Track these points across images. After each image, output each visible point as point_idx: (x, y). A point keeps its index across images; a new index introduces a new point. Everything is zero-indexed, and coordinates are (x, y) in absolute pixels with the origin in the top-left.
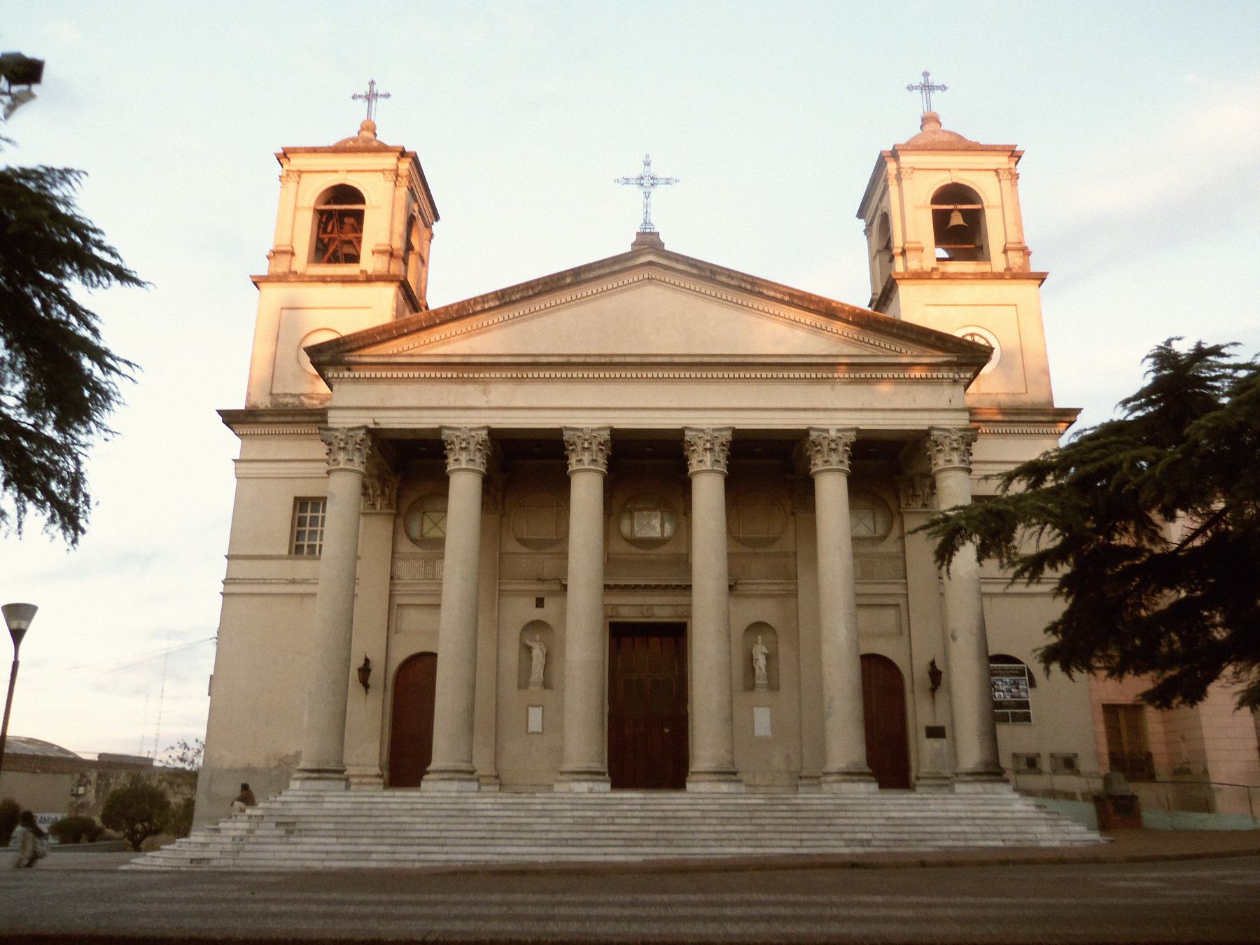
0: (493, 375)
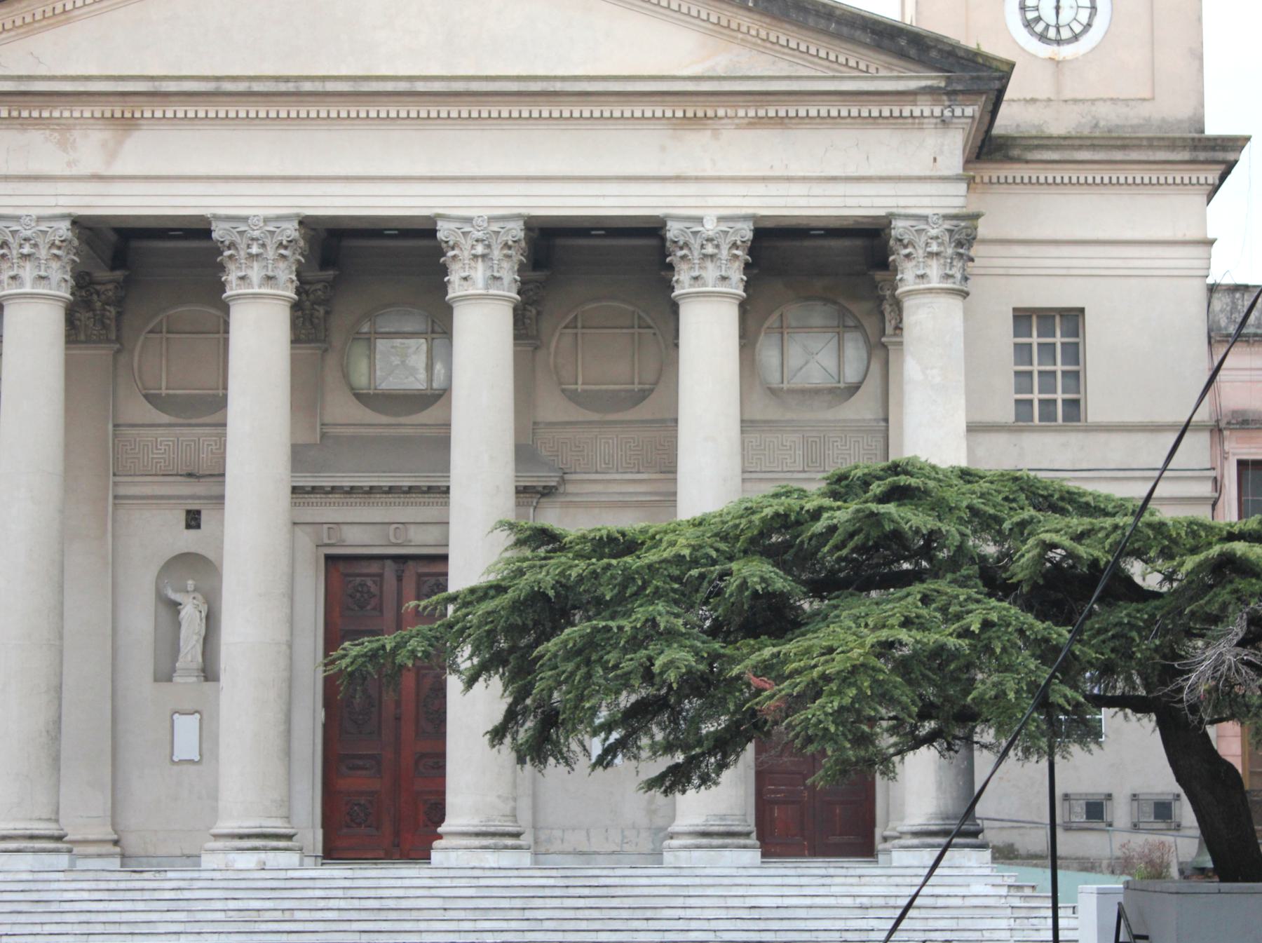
0: (77, 114)
